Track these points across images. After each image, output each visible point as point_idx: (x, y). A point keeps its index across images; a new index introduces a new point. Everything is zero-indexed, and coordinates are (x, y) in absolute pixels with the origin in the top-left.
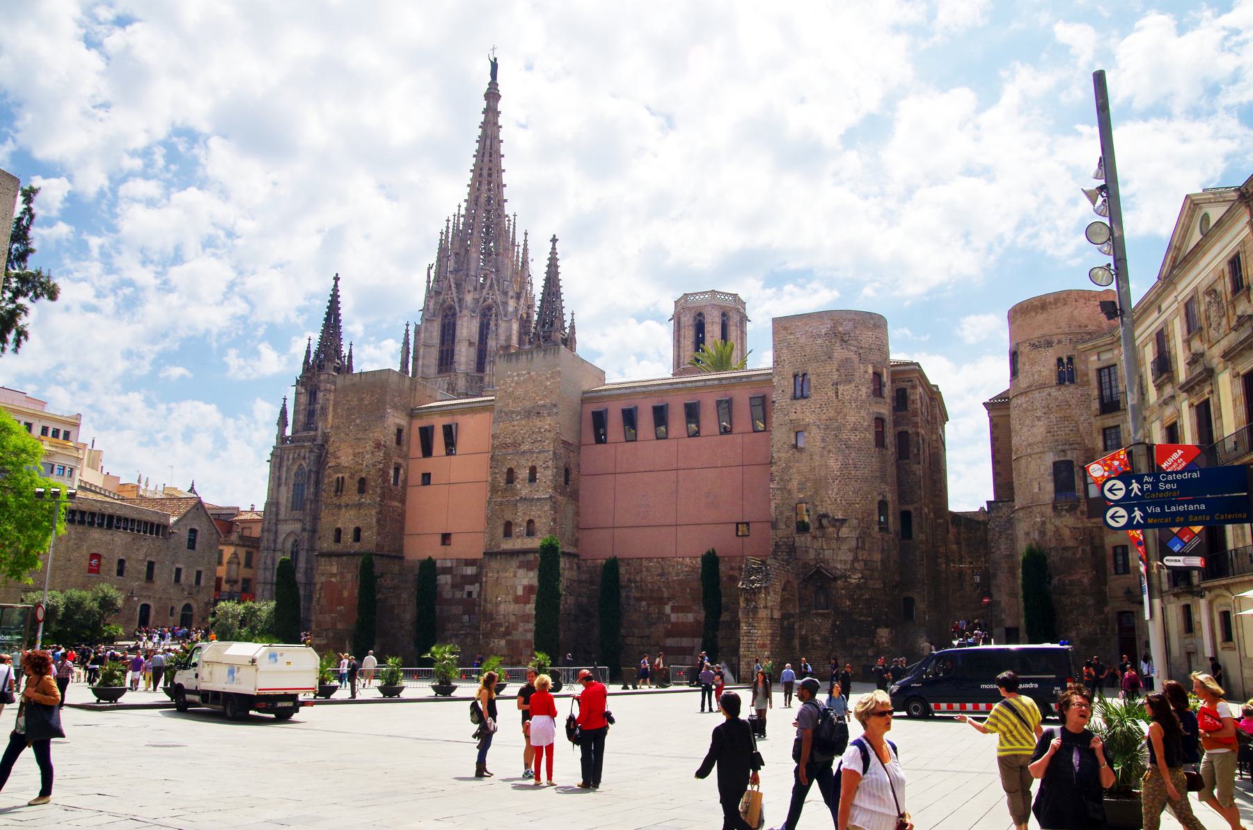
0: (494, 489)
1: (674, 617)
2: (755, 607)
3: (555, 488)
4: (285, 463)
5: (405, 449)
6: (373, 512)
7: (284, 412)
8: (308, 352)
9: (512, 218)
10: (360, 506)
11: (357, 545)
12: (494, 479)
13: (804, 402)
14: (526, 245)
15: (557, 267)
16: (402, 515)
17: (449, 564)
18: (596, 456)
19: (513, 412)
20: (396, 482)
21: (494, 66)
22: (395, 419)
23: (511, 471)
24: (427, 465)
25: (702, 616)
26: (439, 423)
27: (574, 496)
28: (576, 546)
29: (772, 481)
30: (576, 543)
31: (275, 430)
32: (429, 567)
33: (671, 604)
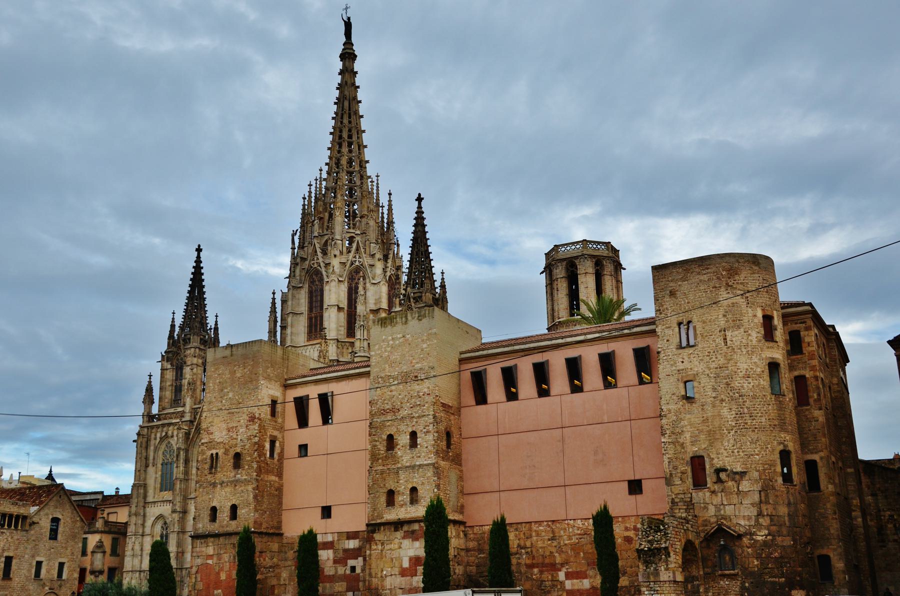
0: (374, 457)
2: (656, 569)
3: (437, 453)
4: (152, 442)
5: (280, 420)
6: (250, 488)
7: (149, 390)
8: (173, 326)
9: (375, 179)
10: (235, 483)
11: (234, 523)
13: (691, 350)
14: (390, 206)
15: (424, 226)
16: (280, 489)
17: (330, 538)
18: (477, 417)
20: (272, 455)
21: (348, 25)
22: (269, 390)
23: (390, 438)
25: (598, 581)
26: (313, 392)
27: (457, 460)
28: (462, 513)
29: (663, 435)
30: (461, 509)
31: (140, 409)
32: (309, 544)
33: (564, 570)
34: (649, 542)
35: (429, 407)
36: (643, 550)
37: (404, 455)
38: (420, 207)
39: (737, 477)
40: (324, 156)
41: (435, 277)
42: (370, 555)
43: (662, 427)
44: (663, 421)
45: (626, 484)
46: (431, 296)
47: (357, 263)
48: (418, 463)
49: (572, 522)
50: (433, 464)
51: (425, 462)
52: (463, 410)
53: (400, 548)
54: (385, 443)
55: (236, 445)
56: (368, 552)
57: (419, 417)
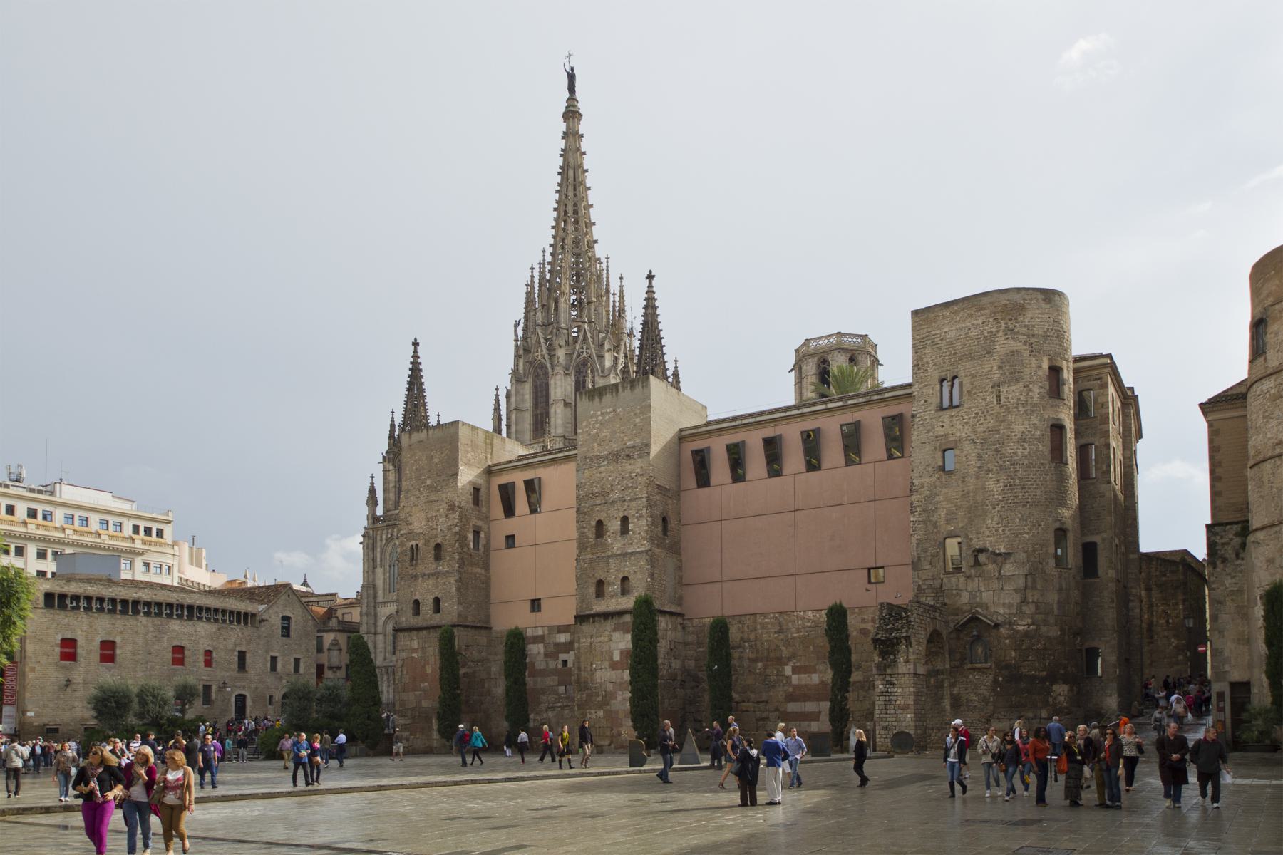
0: (582, 545)
3: (651, 539)
5: (484, 510)
6: (452, 580)
9: (603, 260)
10: (436, 575)
12: (582, 535)
16: (487, 582)
18: (697, 501)
19: (598, 457)
23: (600, 523)
24: (510, 526)
26: (519, 478)
28: (680, 605)
30: (679, 601)
35: (641, 491)
37: (614, 543)
39: (1000, 559)
40: (547, 237)
52: (682, 494)
55: (436, 536)
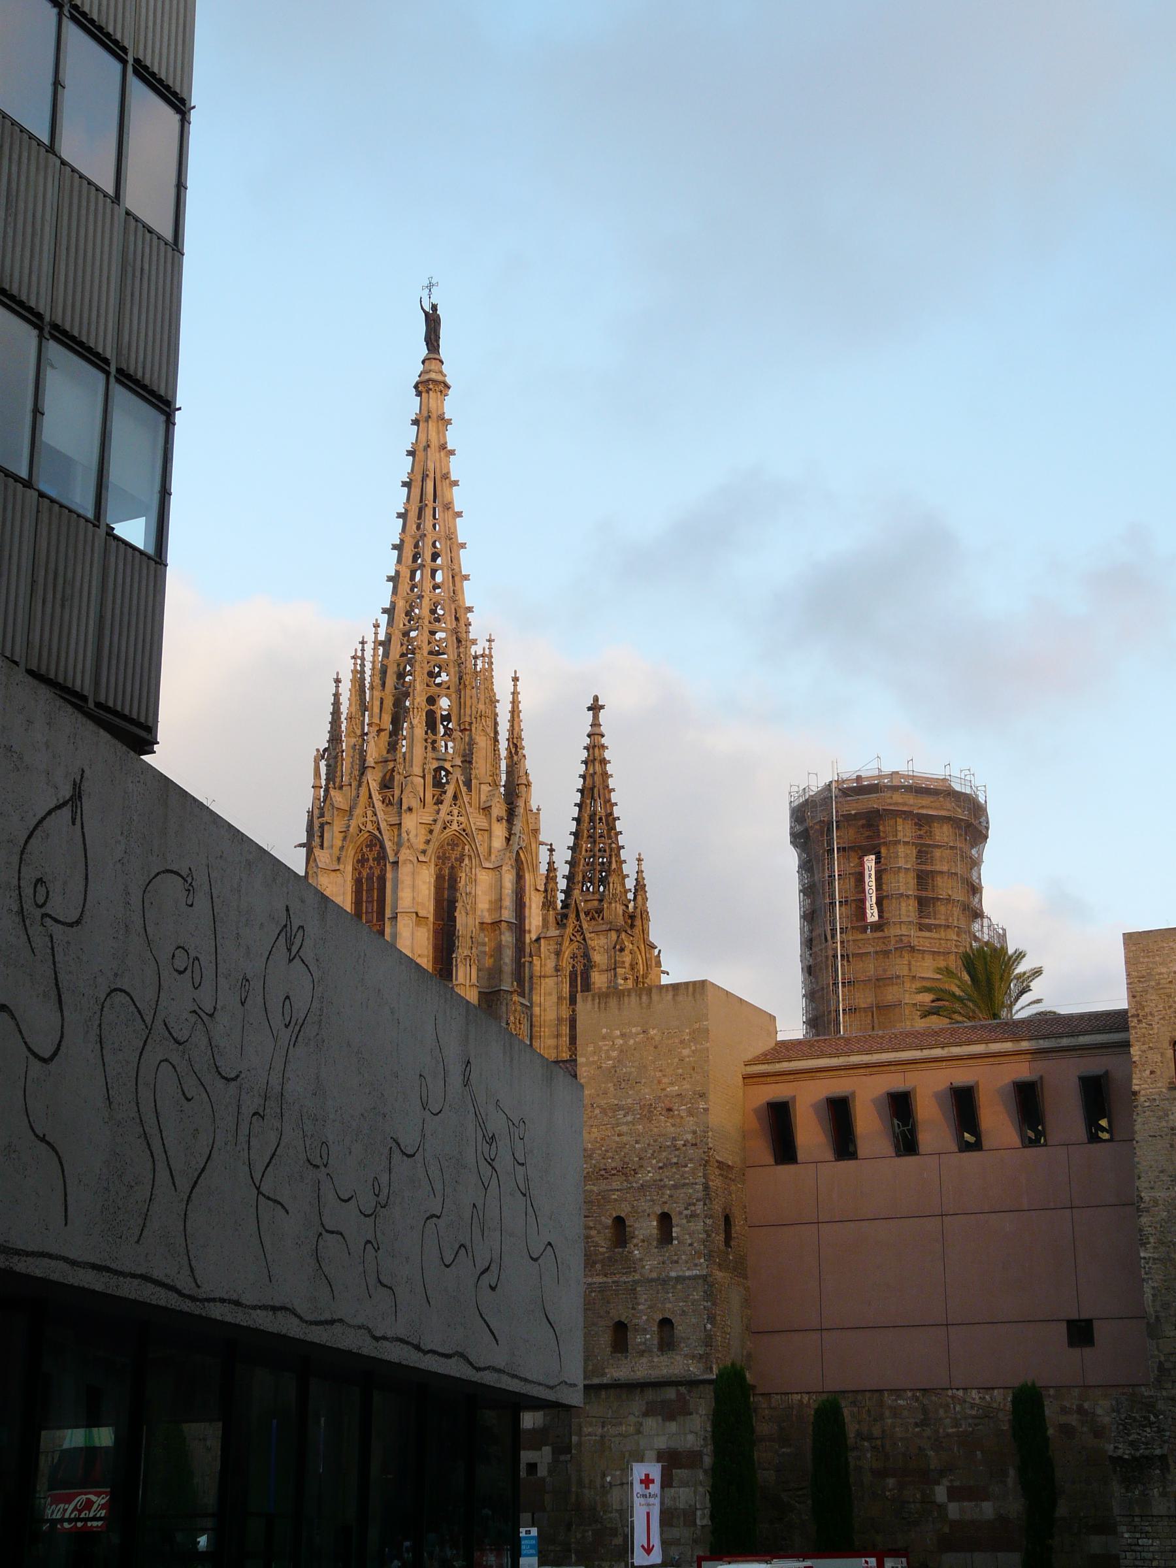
1: (954, 1510)
3: (709, 1257)
14: (515, 703)
19: (619, 1108)
21: (432, 321)
25: (1015, 1507)
29: (1144, 1244)
33: (946, 1482)
34: (1132, 1444)
35: (693, 1172)
36: (1120, 1458)
37: (647, 1259)
38: (595, 724)
41: (626, 869)
42: (580, 1444)
43: (1141, 1230)
44: (1144, 1220)
45: (1064, 1325)
46: (620, 909)
47: (455, 826)
48: (673, 1274)
49: (960, 1393)
50: (704, 1278)
51: (688, 1273)
53: (639, 1432)
54: (608, 1233)
56: (575, 1439)
57: (675, 1187)
